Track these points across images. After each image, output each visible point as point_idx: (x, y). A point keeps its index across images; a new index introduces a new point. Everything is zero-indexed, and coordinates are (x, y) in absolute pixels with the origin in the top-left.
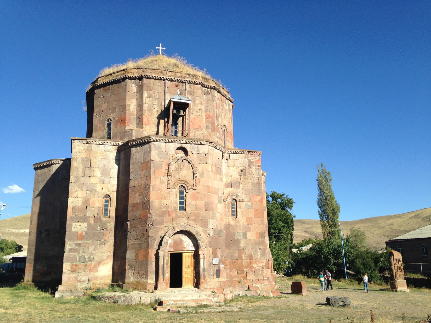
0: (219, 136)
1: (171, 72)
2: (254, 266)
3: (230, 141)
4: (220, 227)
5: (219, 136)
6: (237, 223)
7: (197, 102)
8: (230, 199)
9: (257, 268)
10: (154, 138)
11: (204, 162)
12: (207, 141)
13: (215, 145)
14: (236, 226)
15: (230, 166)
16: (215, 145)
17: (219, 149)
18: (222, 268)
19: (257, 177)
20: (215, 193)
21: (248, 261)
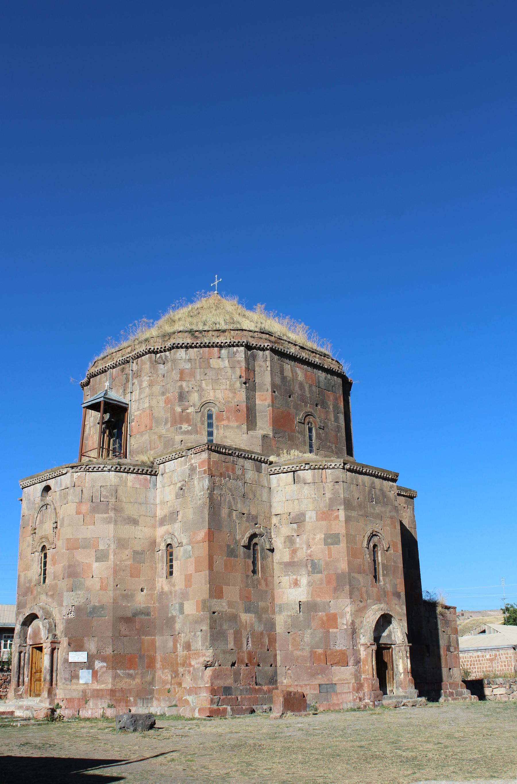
0: (190, 428)
1: (121, 350)
2: (193, 663)
3: (235, 424)
4: (99, 601)
5: (190, 428)
6: (173, 588)
7: (145, 384)
8: (163, 546)
9: (196, 666)
10: (22, 483)
11: (65, 502)
12: (67, 466)
13: (87, 468)
14: (171, 592)
15: (166, 485)
16: (87, 468)
17: (100, 469)
18: (101, 667)
19: (200, 494)
20: (84, 547)
21: (185, 655)
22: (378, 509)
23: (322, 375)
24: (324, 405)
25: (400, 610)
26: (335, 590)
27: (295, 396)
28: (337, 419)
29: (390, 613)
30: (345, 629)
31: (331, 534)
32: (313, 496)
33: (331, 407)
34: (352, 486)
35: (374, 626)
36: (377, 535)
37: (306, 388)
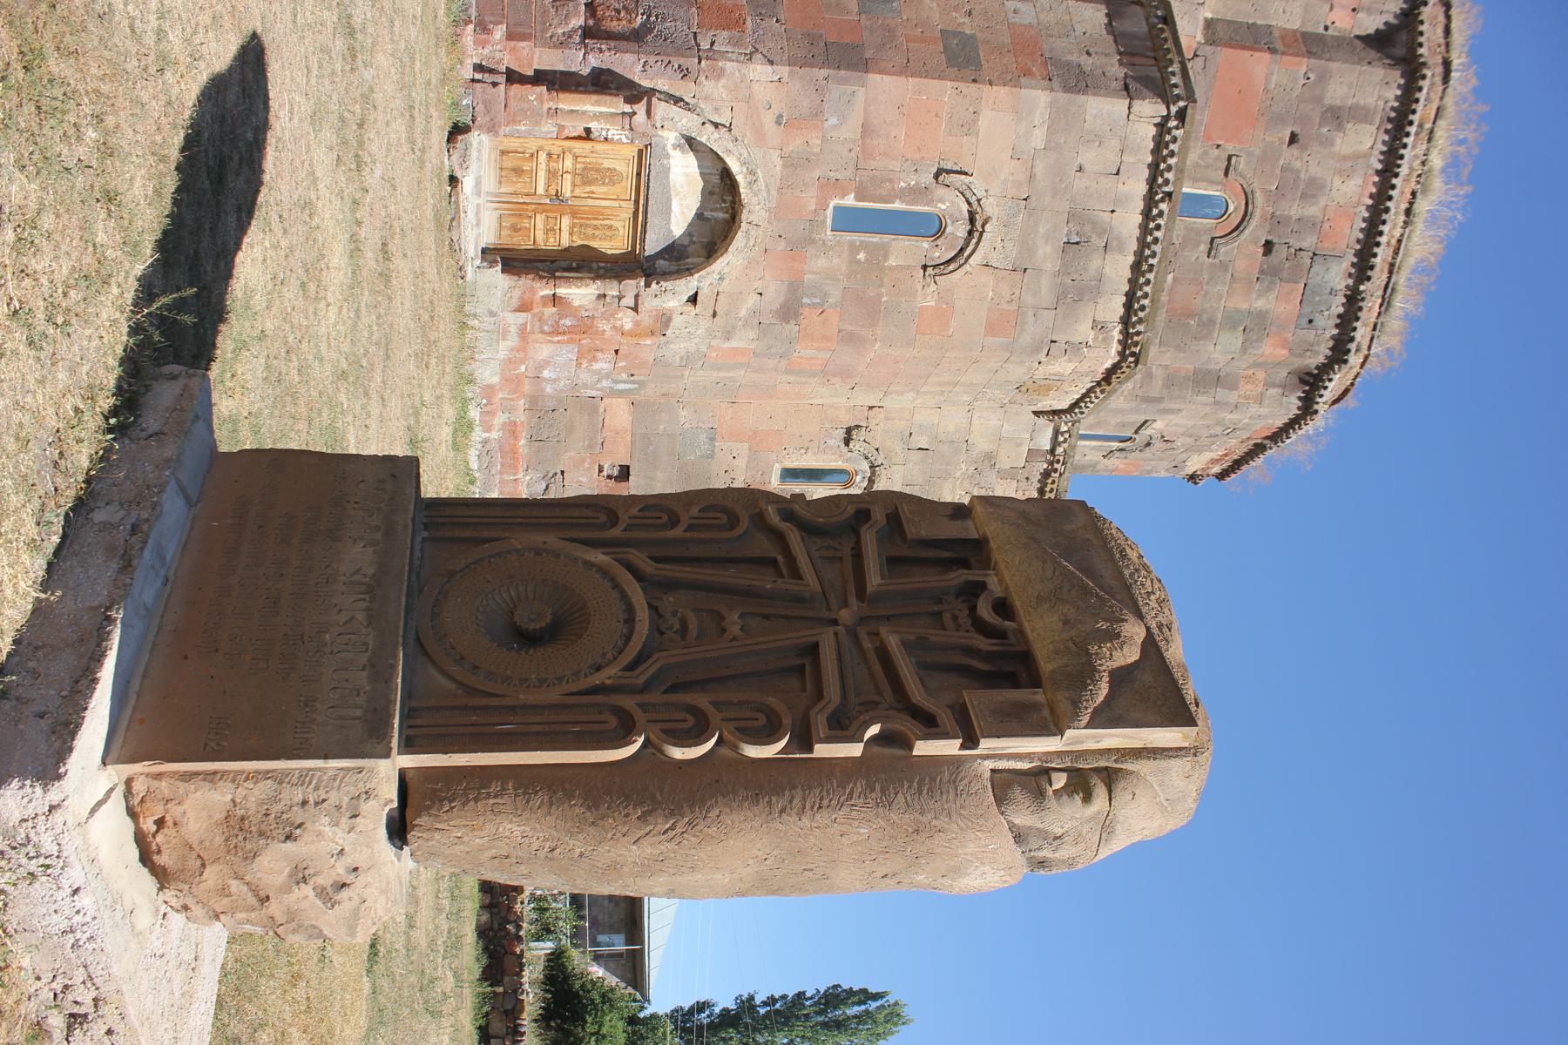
22: (1047, 255)
23: (1337, 276)
24: (1269, 275)
25: (743, 313)
26: (812, 39)
27: (1289, 155)
28: (1231, 322)
29: (740, 233)
30: (698, 45)
31: (976, 50)
32: (1079, 29)
33: (1260, 304)
34: (1115, 144)
35: (703, 140)
36: (970, 233)
37: (1314, 208)
